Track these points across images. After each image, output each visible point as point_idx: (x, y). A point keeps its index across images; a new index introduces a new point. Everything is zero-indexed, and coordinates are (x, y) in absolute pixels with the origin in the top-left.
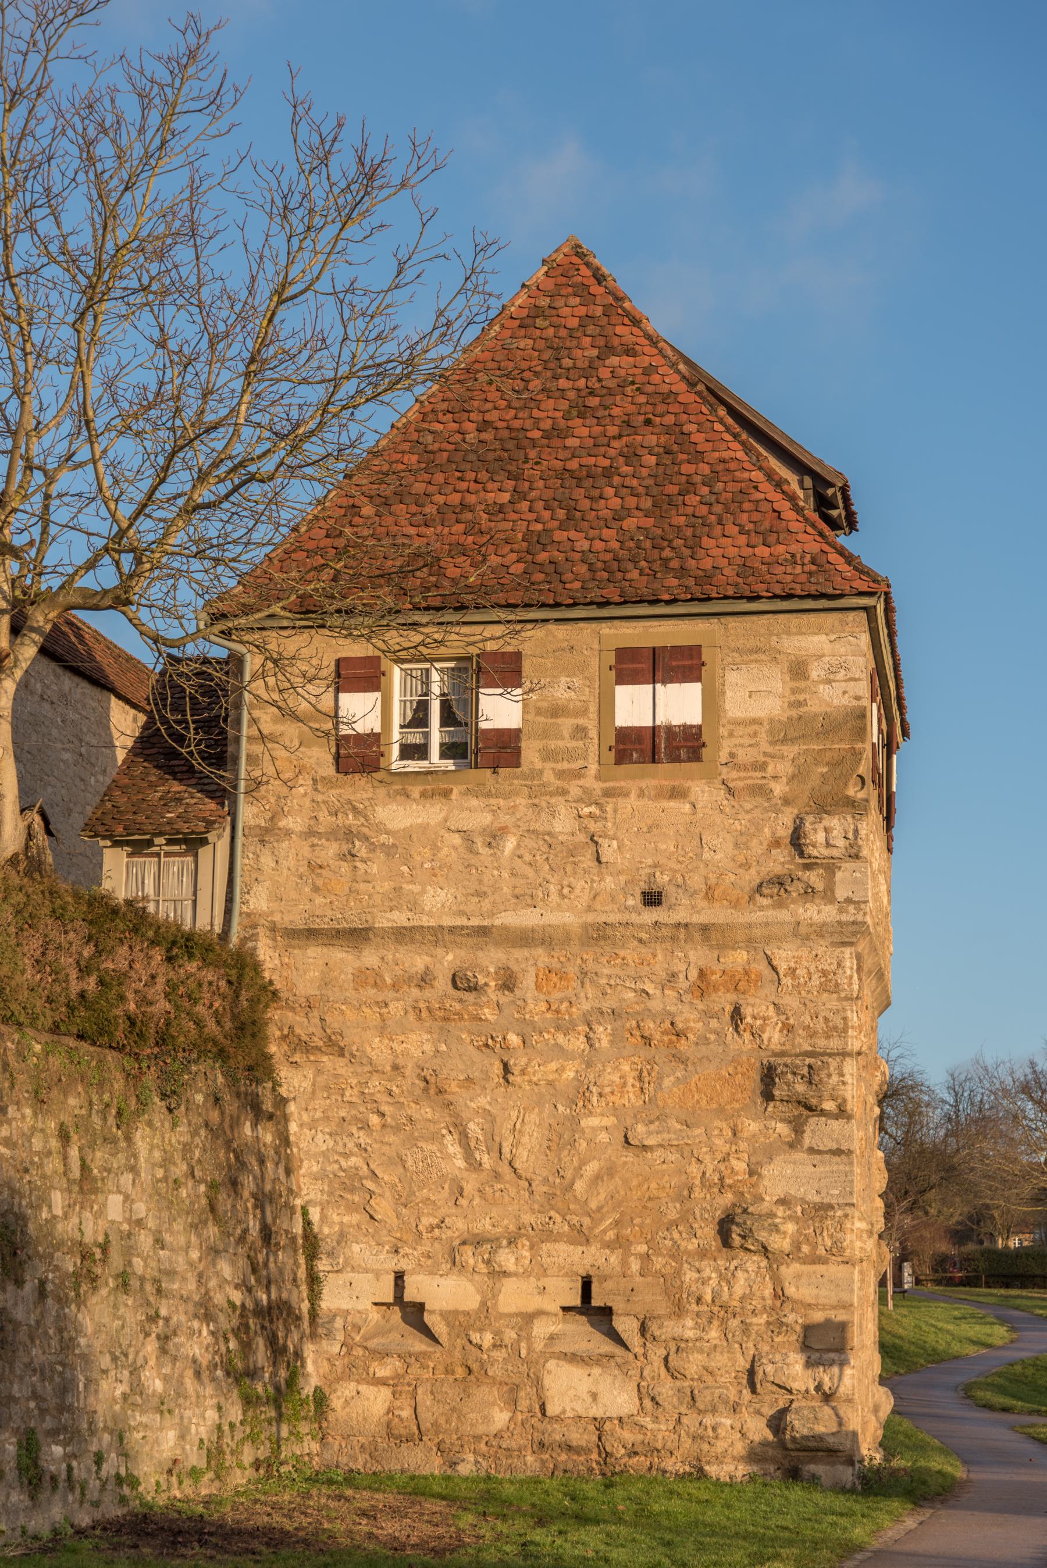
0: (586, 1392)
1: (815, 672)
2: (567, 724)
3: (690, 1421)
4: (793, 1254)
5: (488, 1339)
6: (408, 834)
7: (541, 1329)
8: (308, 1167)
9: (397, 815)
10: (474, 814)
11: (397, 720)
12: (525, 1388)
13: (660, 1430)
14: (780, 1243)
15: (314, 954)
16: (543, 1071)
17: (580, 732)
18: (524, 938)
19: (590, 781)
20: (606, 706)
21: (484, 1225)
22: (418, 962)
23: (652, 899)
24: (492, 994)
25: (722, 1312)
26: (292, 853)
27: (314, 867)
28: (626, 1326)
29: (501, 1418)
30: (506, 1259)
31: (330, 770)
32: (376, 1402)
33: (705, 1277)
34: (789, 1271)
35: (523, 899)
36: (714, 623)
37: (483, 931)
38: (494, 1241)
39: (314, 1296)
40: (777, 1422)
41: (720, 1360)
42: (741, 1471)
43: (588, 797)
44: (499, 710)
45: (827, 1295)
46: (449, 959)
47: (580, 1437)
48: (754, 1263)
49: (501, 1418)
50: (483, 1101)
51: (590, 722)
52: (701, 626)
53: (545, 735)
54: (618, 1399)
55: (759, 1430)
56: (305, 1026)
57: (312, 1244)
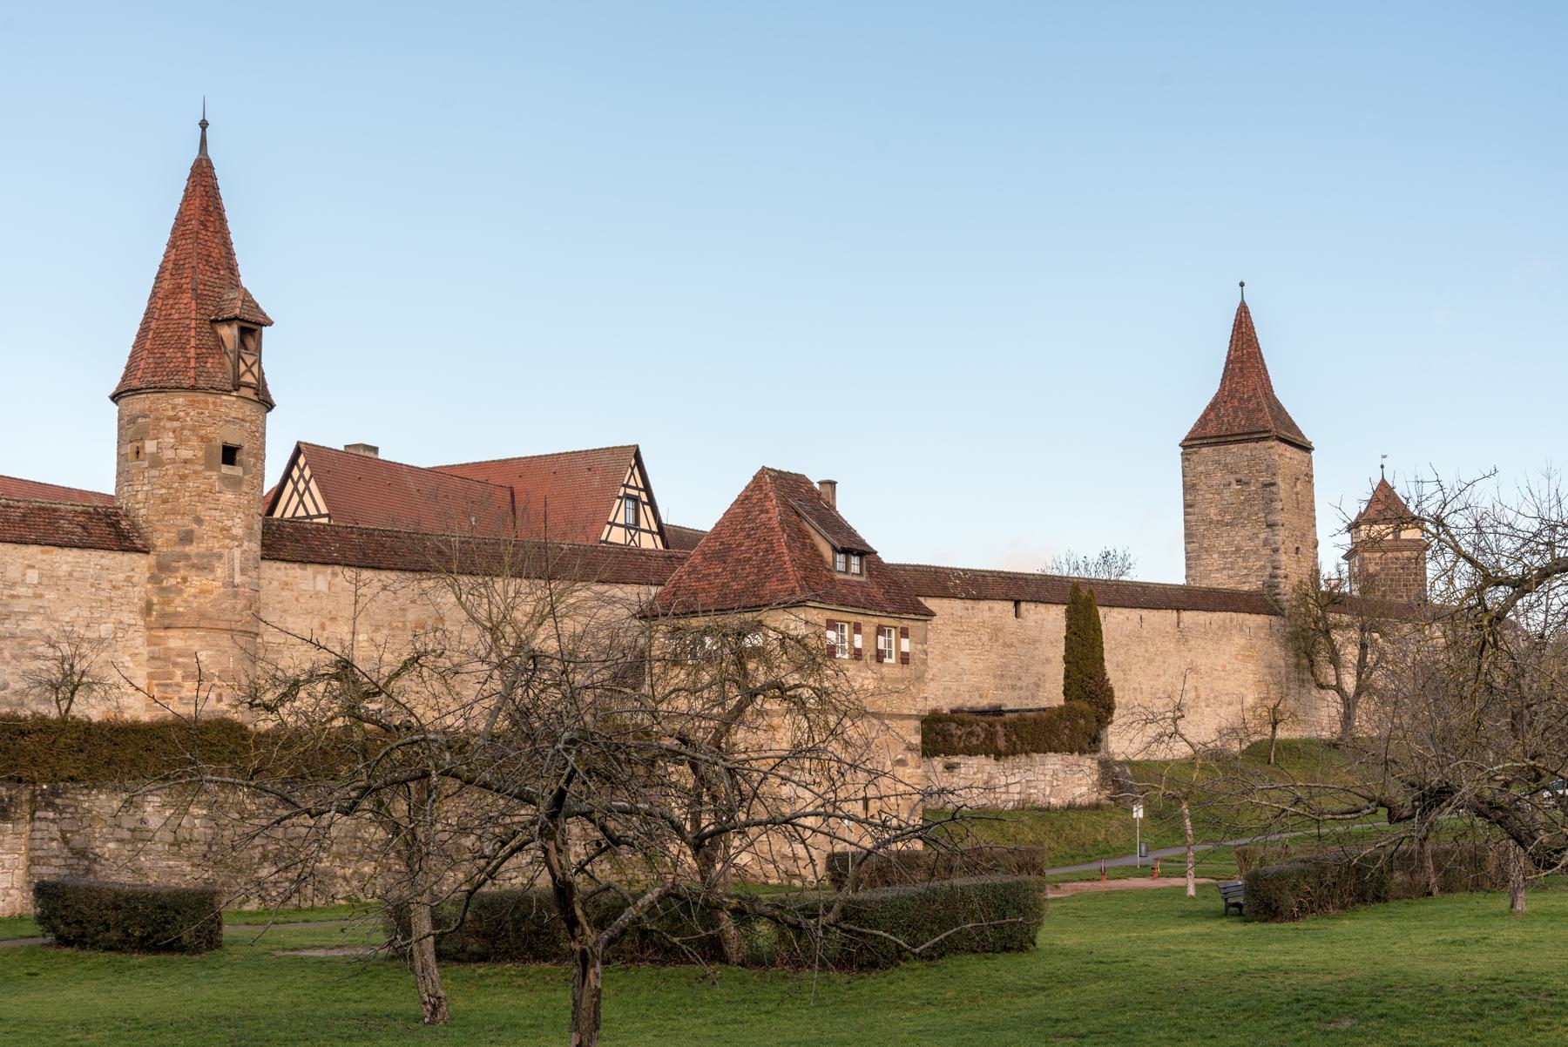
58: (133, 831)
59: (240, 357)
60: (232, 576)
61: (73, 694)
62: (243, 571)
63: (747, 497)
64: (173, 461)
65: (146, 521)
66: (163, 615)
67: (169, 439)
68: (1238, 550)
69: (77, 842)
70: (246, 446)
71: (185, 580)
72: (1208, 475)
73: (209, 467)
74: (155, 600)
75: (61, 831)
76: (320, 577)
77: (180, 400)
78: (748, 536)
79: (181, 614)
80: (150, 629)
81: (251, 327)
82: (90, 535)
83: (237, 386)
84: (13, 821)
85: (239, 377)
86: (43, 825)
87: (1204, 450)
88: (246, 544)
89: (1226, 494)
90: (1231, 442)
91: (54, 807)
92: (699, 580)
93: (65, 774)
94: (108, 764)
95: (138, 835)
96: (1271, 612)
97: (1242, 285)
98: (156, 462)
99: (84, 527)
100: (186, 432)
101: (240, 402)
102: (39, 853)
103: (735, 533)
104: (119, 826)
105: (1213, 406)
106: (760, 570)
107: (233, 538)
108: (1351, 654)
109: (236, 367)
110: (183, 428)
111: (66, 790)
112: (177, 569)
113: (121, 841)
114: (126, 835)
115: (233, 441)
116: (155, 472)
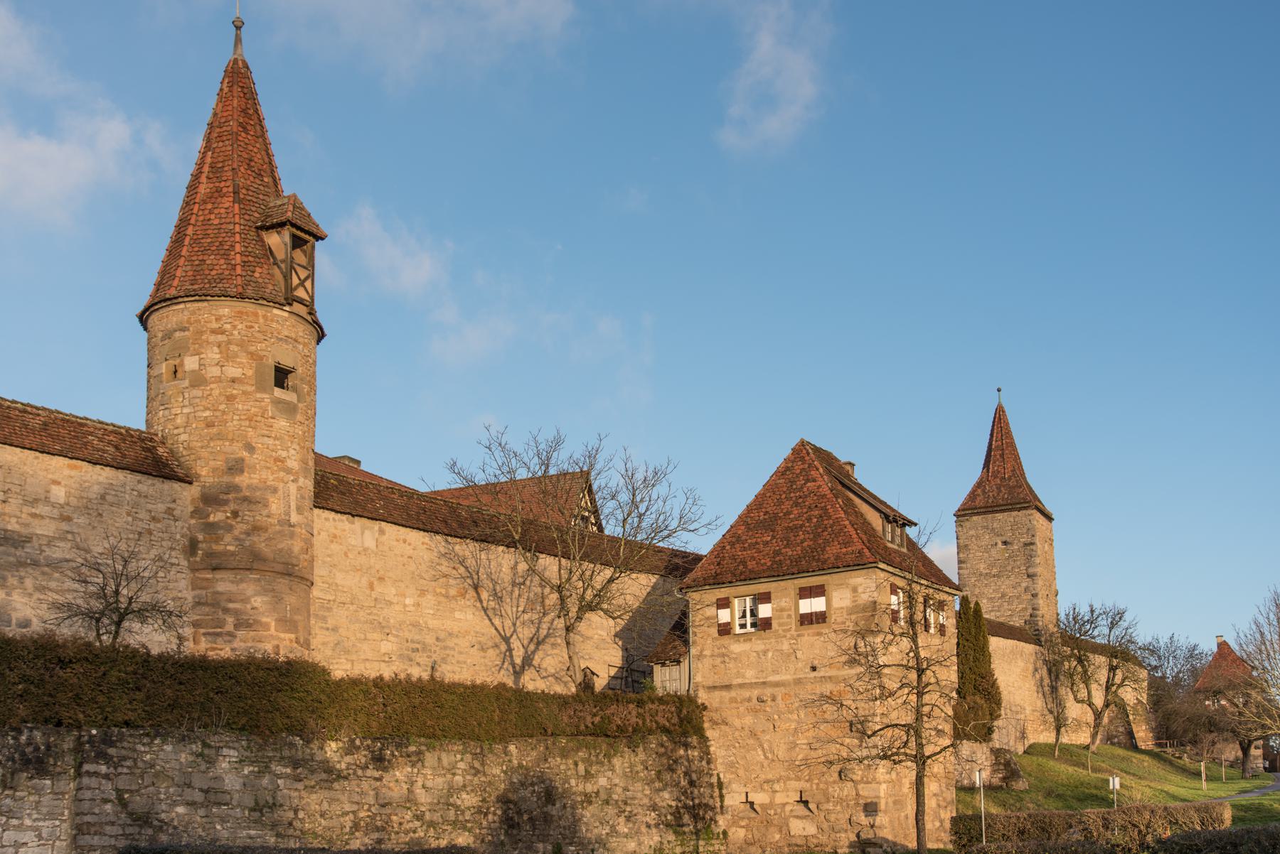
0: (802, 828)
1: (860, 590)
2: (785, 614)
3: (833, 836)
4: (861, 781)
5: (772, 812)
6: (740, 654)
7: (788, 808)
8: (720, 761)
9: (737, 647)
10: (758, 645)
11: (737, 615)
12: (783, 827)
13: (823, 839)
14: (855, 777)
15: (717, 693)
16: (784, 726)
17: (789, 616)
18: (777, 684)
19: (793, 632)
20: (797, 607)
21: (770, 776)
22: (747, 694)
23: (814, 669)
24: (769, 703)
25: (841, 800)
26: (707, 662)
27: (714, 666)
28: (812, 806)
29: (777, 837)
30: (777, 787)
31: (716, 635)
32: (741, 833)
33: (835, 791)
34: (860, 787)
35: (775, 672)
36: (828, 577)
37: (764, 683)
38: (773, 781)
39: (722, 801)
40: (858, 835)
41: (841, 816)
42: (847, 851)
43: (792, 638)
44: (765, 611)
45: (872, 794)
46: (756, 693)
47: (799, 842)
48: (850, 784)
49: (777, 837)
50: (768, 737)
51: (792, 613)
52: (825, 577)
53: (779, 618)
54: (812, 830)
55: (853, 838)
56: (716, 716)
57: (720, 785)
58: (206, 792)
59: (292, 268)
60: (288, 514)
61: (118, 624)
62: (299, 510)
63: (787, 469)
64: (219, 380)
65: (189, 448)
66: (210, 555)
67: (213, 354)
68: (1003, 596)
69: (138, 803)
70: (300, 370)
71: (235, 514)
72: (978, 537)
73: (261, 388)
74: (200, 537)
75: (117, 790)
76: (367, 532)
77: (226, 309)
78: (797, 504)
79: (233, 554)
80: (194, 570)
81: (306, 237)
82: (124, 456)
83: (290, 300)
84: (54, 776)
85: (293, 290)
86: (93, 782)
87: (975, 518)
88: (301, 480)
89: (993, 552)
90: (997, 512)
91: (107, 759)
92: (745, 549)
93: (120, 717)
94: (172, 707)
95: (212, 797)
96: (1038, 642)
97: (999, 390)
98: (198, 380)
99: (116, 447)
100: (234, 348)
101: (293, 319)
102: (88, 818)
103: (780, 503)
104: (189, 786)
105: (979, 484)
106: (817, 535)
107: (289, 471)
108: (1103, 675)
109: (287, 278)
110: (229, 342)
111: (121, 738)
112: (226, 502)
113: (191, 804)
114: (198, 797)
115: (287, 362)
116: (197, 392)
